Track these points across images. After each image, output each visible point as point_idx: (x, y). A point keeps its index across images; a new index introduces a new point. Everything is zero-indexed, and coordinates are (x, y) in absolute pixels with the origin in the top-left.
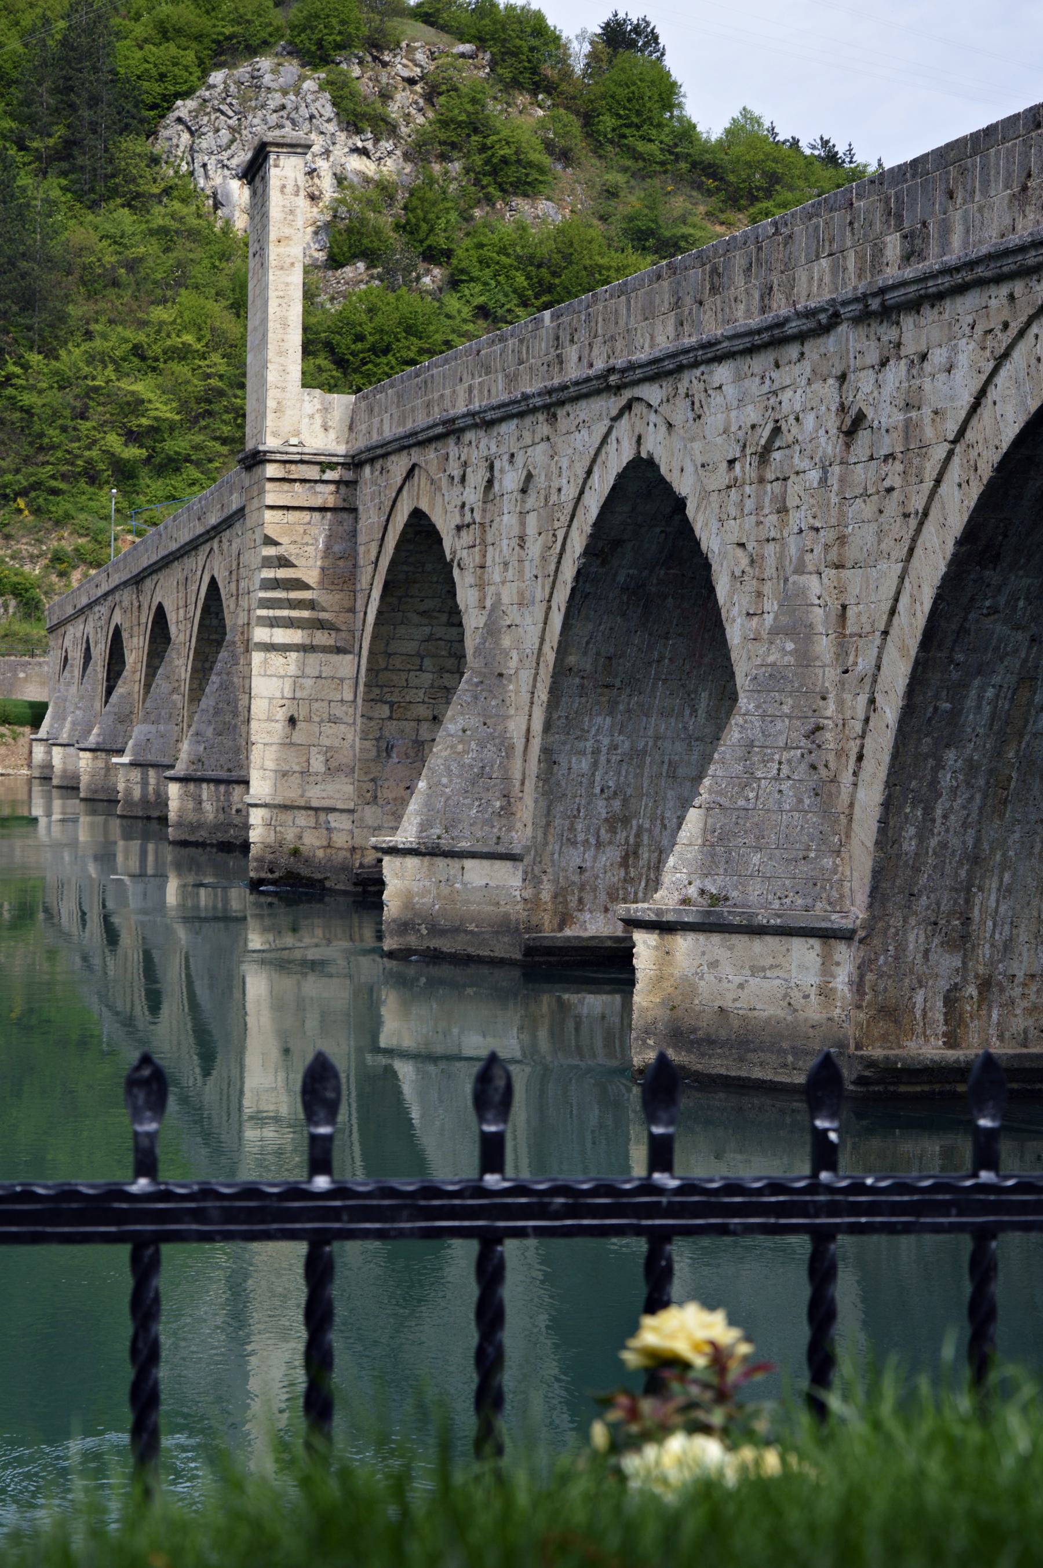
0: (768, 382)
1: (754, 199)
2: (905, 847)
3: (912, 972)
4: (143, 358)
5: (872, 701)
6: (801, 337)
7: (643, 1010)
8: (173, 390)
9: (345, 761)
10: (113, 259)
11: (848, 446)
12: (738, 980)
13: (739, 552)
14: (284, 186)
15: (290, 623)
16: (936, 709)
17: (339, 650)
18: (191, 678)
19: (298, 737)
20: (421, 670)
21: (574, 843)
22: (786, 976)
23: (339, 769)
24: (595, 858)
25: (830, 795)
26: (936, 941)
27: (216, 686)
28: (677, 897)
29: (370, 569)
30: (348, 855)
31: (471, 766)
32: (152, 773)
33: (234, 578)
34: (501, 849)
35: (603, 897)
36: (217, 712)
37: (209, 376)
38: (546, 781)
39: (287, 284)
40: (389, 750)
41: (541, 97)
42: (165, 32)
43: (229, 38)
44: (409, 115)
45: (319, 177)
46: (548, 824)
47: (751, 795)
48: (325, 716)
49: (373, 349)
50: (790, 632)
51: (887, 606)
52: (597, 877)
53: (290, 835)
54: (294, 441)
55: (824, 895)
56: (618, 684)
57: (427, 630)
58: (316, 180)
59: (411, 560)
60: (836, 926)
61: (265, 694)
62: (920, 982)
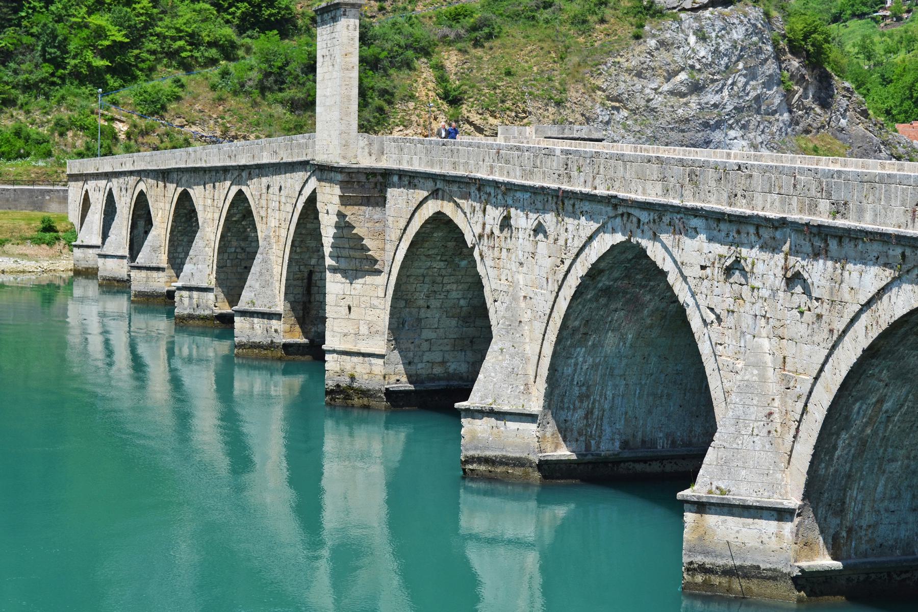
0: (731, 238)
8: (119, 23)
14: (348, 26)
19: (353, 315)
20: (423, 283)
21: (563, 409)
23: (377, 332)
24: (572, 415)
27: (260, 260)
30: (382, 378)
33: (264, 197)
35: (575, 434)
36: (261, 274)
39: (350, 78)
46: (551, 400)
47: (740, 442)
48: (368, 305)
52: (573, 424)
54: (354, 161)
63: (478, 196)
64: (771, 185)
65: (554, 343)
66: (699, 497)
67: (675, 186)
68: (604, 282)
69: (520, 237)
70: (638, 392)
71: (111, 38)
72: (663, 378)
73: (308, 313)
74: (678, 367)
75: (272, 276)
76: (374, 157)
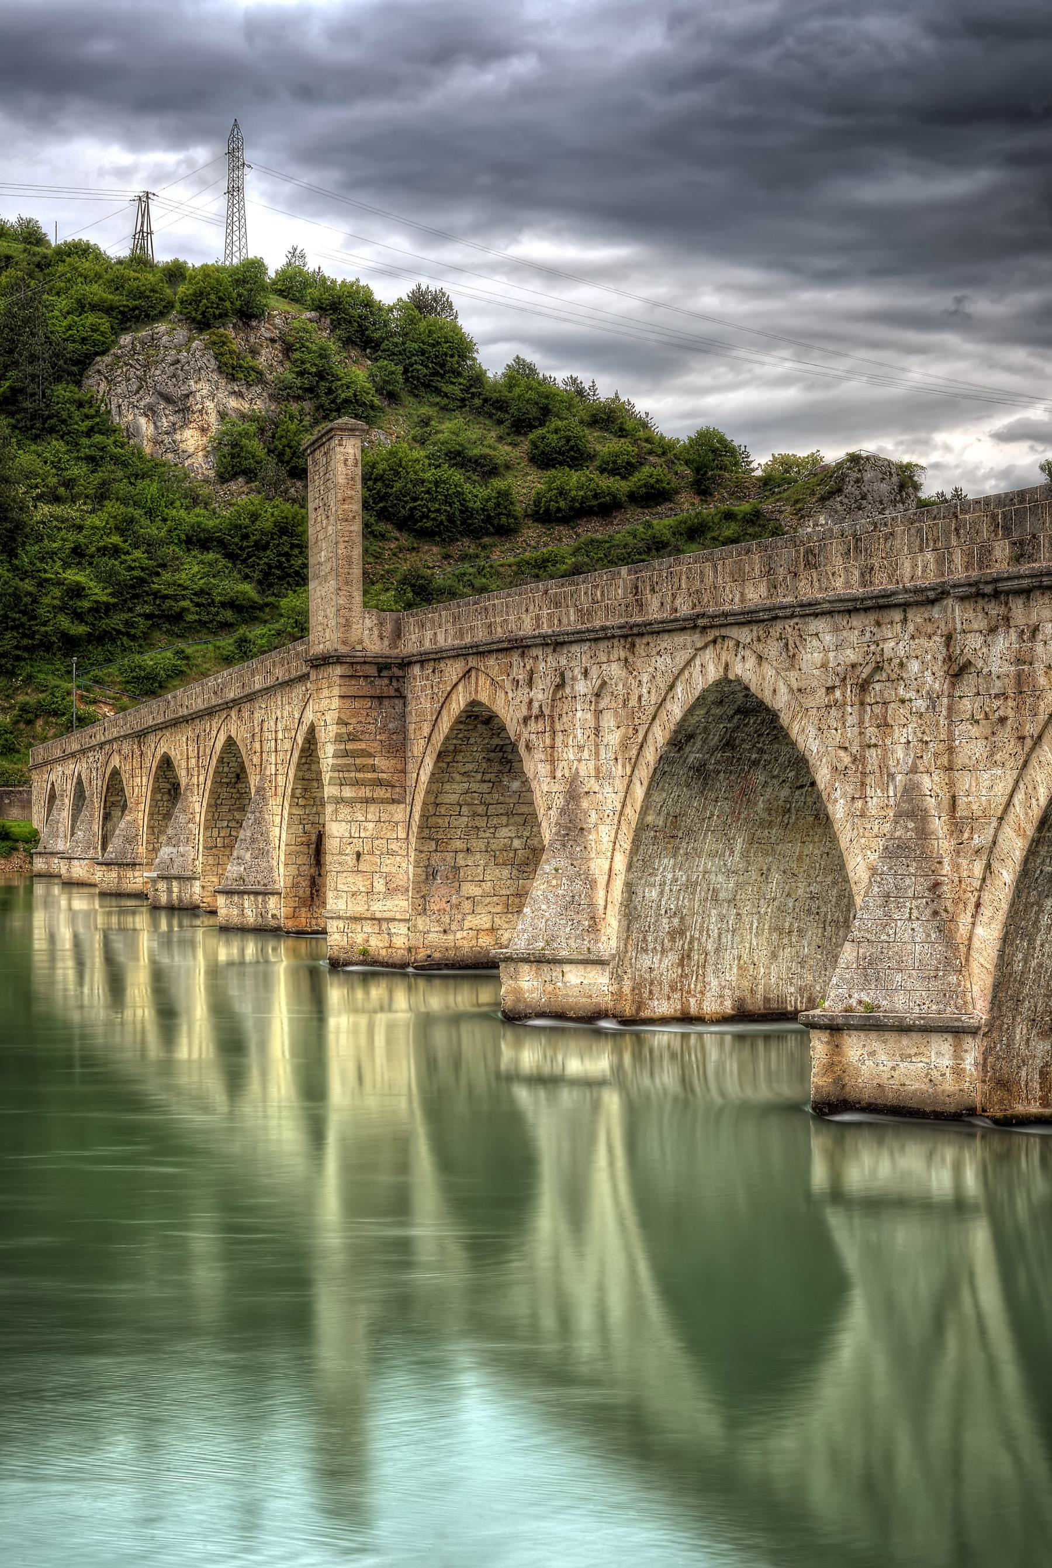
0: (868, 635)
1: (532, 427)
2: (1015, 968)
3: (1018, 1055)
4: (82, 555)
5: (988, 866)
6: (905, 606)
7: (817, 1088)
8: (108, 578)
9: (401, 883)
10: (55, 480)
11: (953, 685)
12: (890, 1064)
13: (842, 753)
14: (346, 460)
15: (357, 783)
16: (1042, 871)
17: (394, 801)
18: (207, 812)
19: (363, 867)
21: (646, 951)
22: (927, 1060)
23: (396, 889)
24: (661, 961)
25: (950, 931)
26: (1034, 1032)
28: (841, 1007)
29: (422, 742)
31: (564, 896)
32: (175, 884)
33: (257, 739)
34: (592, 957)
35: (667, 989)
37: (133, 569)
38: (627, 906)
40: (434, 874)
41: (368, 351)
42: (81, 306)
43: (134, 309)
44: (272, 365)
45: (207, 414)
46: (628, 937)
47: (891, 932)
48: (385, 850)
49: (257, 544)
50: (911, 815)
51: (1004, 800)
53: (359, 939)
55: (952, 1002)
56: (680, 835)
57: (466, 785)
58: (205, 416)
59: (460, 736)
60: (965, 1025)
61: (337, 834)
62: (1023, 1061)
63: (522, 664)
64: (922, 540)
65: (627, 852)
66: (832, 1018)
67: (785, 579)
68: (694, 755)
69: (579, 708)
70: (755, 925)
71: (94, 598)
72: (791, 905)
73: (317, 891)
74: (812, 888)
75: (267, 842)
76: (386, 642)
